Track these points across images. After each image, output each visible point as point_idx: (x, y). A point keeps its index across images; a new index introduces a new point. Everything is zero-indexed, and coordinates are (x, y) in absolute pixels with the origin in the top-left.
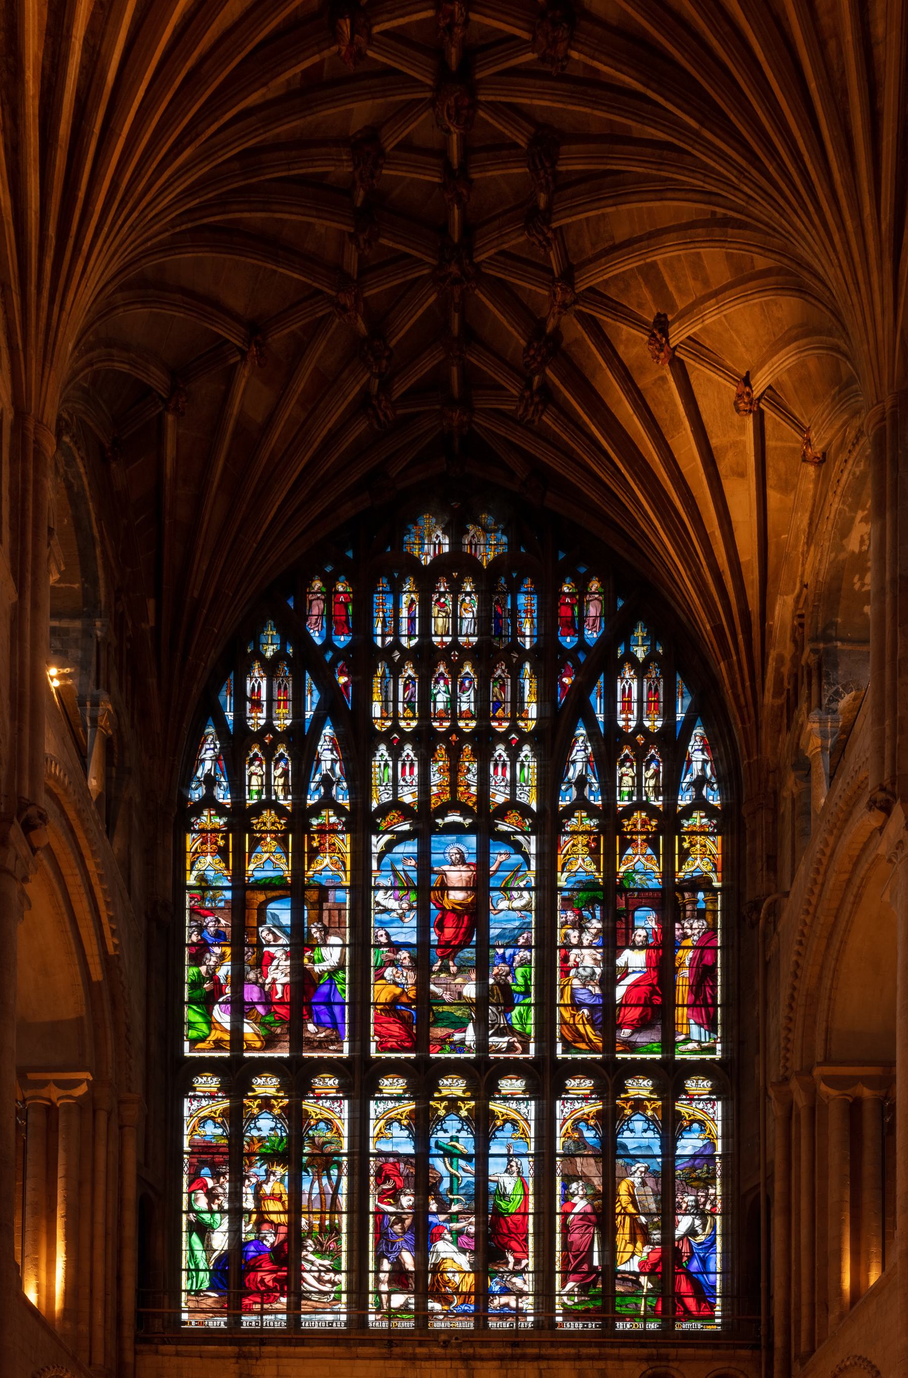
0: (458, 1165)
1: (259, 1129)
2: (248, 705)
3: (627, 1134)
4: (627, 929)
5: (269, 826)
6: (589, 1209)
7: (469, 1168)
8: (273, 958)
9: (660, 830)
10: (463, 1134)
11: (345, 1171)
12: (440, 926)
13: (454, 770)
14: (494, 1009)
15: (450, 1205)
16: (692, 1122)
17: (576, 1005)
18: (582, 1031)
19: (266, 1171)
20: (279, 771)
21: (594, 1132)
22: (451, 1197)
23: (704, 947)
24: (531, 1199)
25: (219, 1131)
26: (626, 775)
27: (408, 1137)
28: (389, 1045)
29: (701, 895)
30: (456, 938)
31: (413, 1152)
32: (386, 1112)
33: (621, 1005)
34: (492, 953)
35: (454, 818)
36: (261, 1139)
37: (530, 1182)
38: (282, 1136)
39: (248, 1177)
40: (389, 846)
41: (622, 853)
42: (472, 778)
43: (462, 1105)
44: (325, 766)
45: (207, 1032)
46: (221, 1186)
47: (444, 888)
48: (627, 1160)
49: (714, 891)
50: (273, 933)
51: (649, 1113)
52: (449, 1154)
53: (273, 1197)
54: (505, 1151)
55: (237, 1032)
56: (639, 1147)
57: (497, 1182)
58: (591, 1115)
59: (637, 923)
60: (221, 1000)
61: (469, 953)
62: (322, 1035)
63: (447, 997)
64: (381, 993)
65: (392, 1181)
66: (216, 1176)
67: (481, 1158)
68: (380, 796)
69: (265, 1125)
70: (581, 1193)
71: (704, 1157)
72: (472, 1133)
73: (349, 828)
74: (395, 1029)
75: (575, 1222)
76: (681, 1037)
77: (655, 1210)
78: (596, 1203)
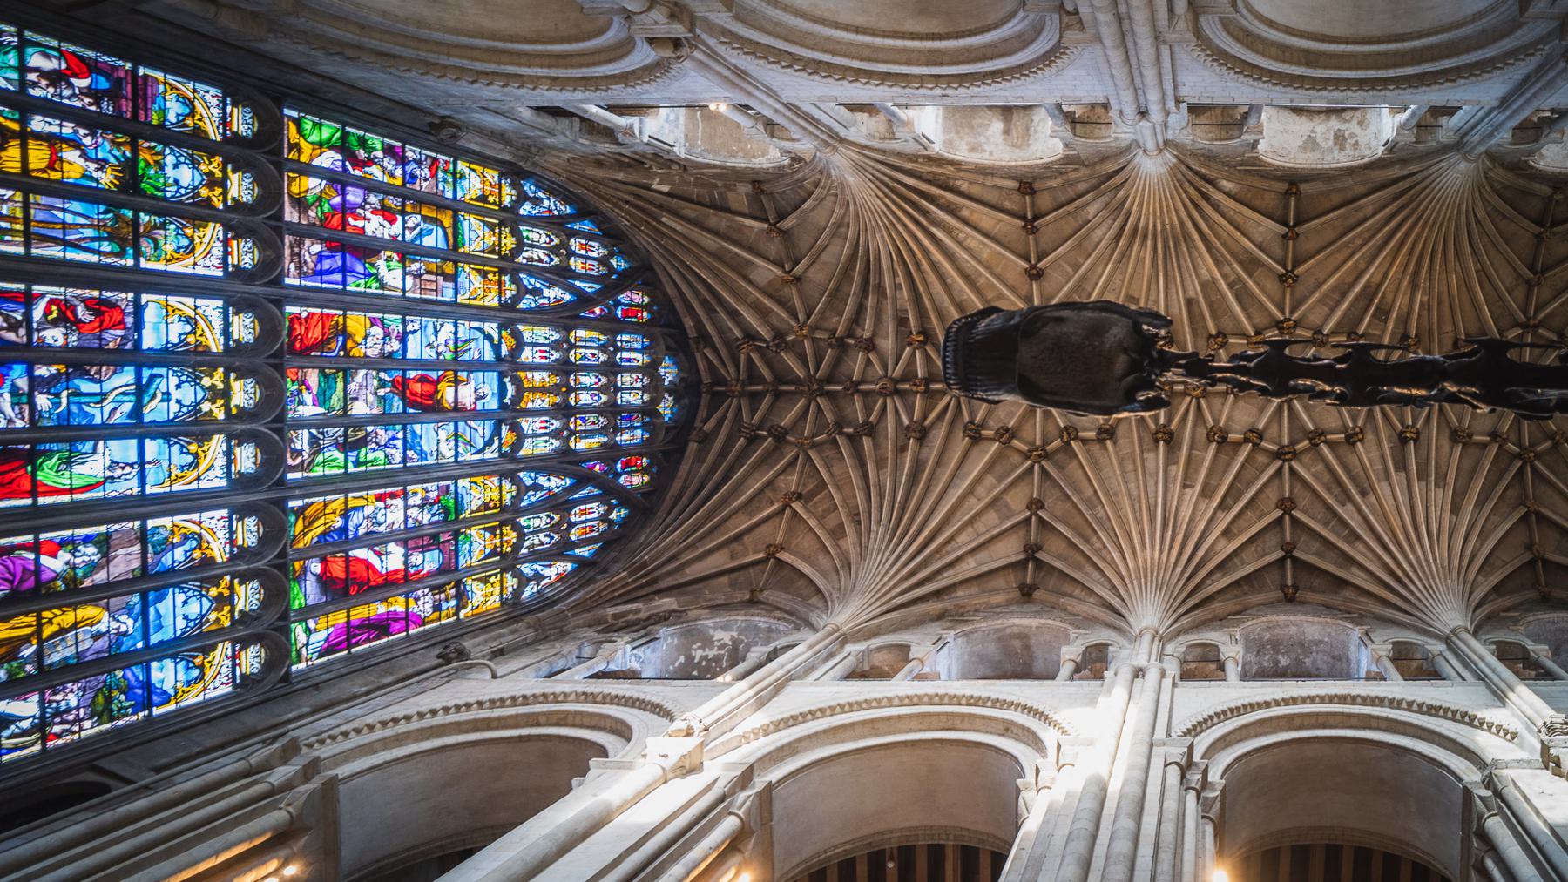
0: (123, 402)
1: (176, 166)
2: (583, 242)
3: (181, 597)
4: (423, 546)
5: (503, 241)
6: (45, 576)
7: (118, 414)
8: (392, 222)
9: (503, 556)
10: (174, 407)
11: (108, 260)
12: (423, 380)
13: (544, 390)
14: (340, 433)
15: (48, 393)
16: (202, 667)
17: (346, 515)
18: (316, 525)
19: (106, 161)
20: (542, 257)
21: (182, 559)
22: (64, 394)
23: (409, 619)
24: (66, 498)
25: (172, 117)
26: (541, 521)
27: (168, 342)
28: (296, 326)
29: (453, 603)
30: (412, 394)
31: (145, 346)
32: (206, 318)
33: (348, 556)
34: (398, 427)
35: (511, 390)
36: (161, 166)
37: (98, 494)
38: (164, 191)
39: (93, 134)
40: (489, 337)
41: (485, 529)
42: (538, 404)
43: (218, 405)
44: (546, 292)
45: (310, 139)
46: (74, 95)
47: (457, 382)
48: (138, 608)
49: (456, 613)
50: (415, 228)
51: (212, 616)
52: (140, 390)
53: (54, 162)
54: (148, 458)
55: (308, 170)
56: (159, 616)
57: (94, 451)
58: (207, 552)
59: (428, 554)
60: (347, 163)
61: (397, 406)
62: (307, 258)
63: (352, 386)
64: (356, 322)
65: (92, 318)
66: (95, 94)
67: (138, 428)
68: (527, 332)
69: (185, 175)
70: (78, 561)
71: (148, 694)
72: (176, 417)
73: (504, 306)
74: (316, 334)
75: (19, 562)
76: (311, 624)
77: (48, 662)
78: (59, 583)
